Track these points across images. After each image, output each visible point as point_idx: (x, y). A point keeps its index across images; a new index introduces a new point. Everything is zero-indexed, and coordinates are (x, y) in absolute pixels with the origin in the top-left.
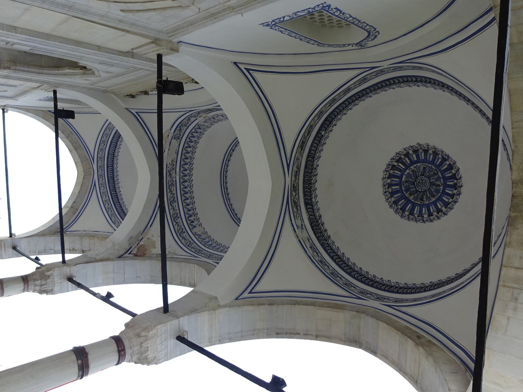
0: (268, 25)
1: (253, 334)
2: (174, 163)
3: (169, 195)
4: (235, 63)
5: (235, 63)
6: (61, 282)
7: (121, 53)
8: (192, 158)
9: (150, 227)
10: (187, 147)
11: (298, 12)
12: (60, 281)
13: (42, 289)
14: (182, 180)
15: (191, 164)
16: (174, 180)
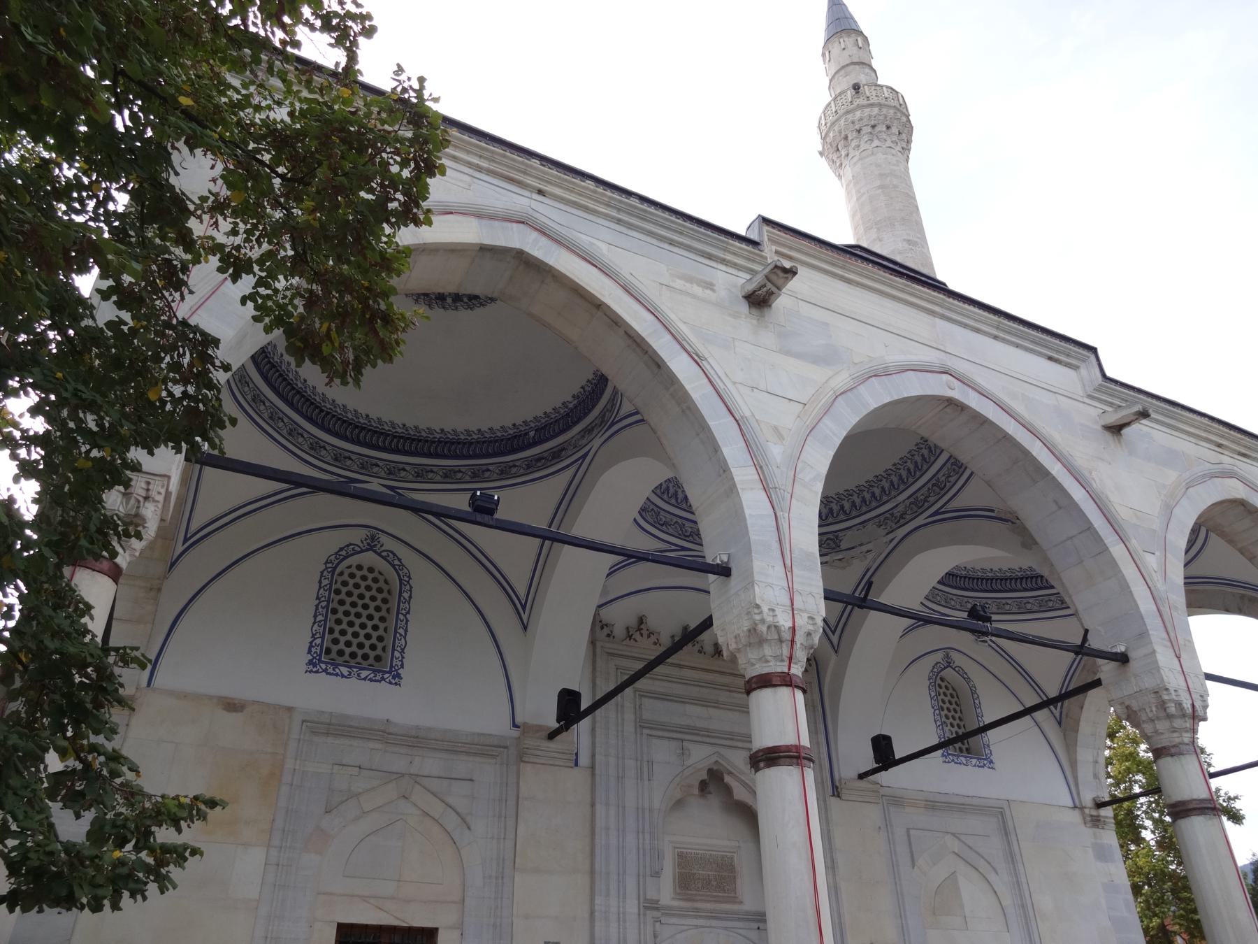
0: (399, 676)
1: (689, 408)
2: (882, 518)
3: (932, 499)
4: (525, 628)
5: (525, 628)
6: (1136, 676)
7: (593, 775)
8: (860, 489)
9: (993, 511)
10: (845, 512)
11: (343, 676)
12: (1133, 679)
13: (1162, 714)
14: (902, 487)
15: (870, 485)
16: (907, 502)
